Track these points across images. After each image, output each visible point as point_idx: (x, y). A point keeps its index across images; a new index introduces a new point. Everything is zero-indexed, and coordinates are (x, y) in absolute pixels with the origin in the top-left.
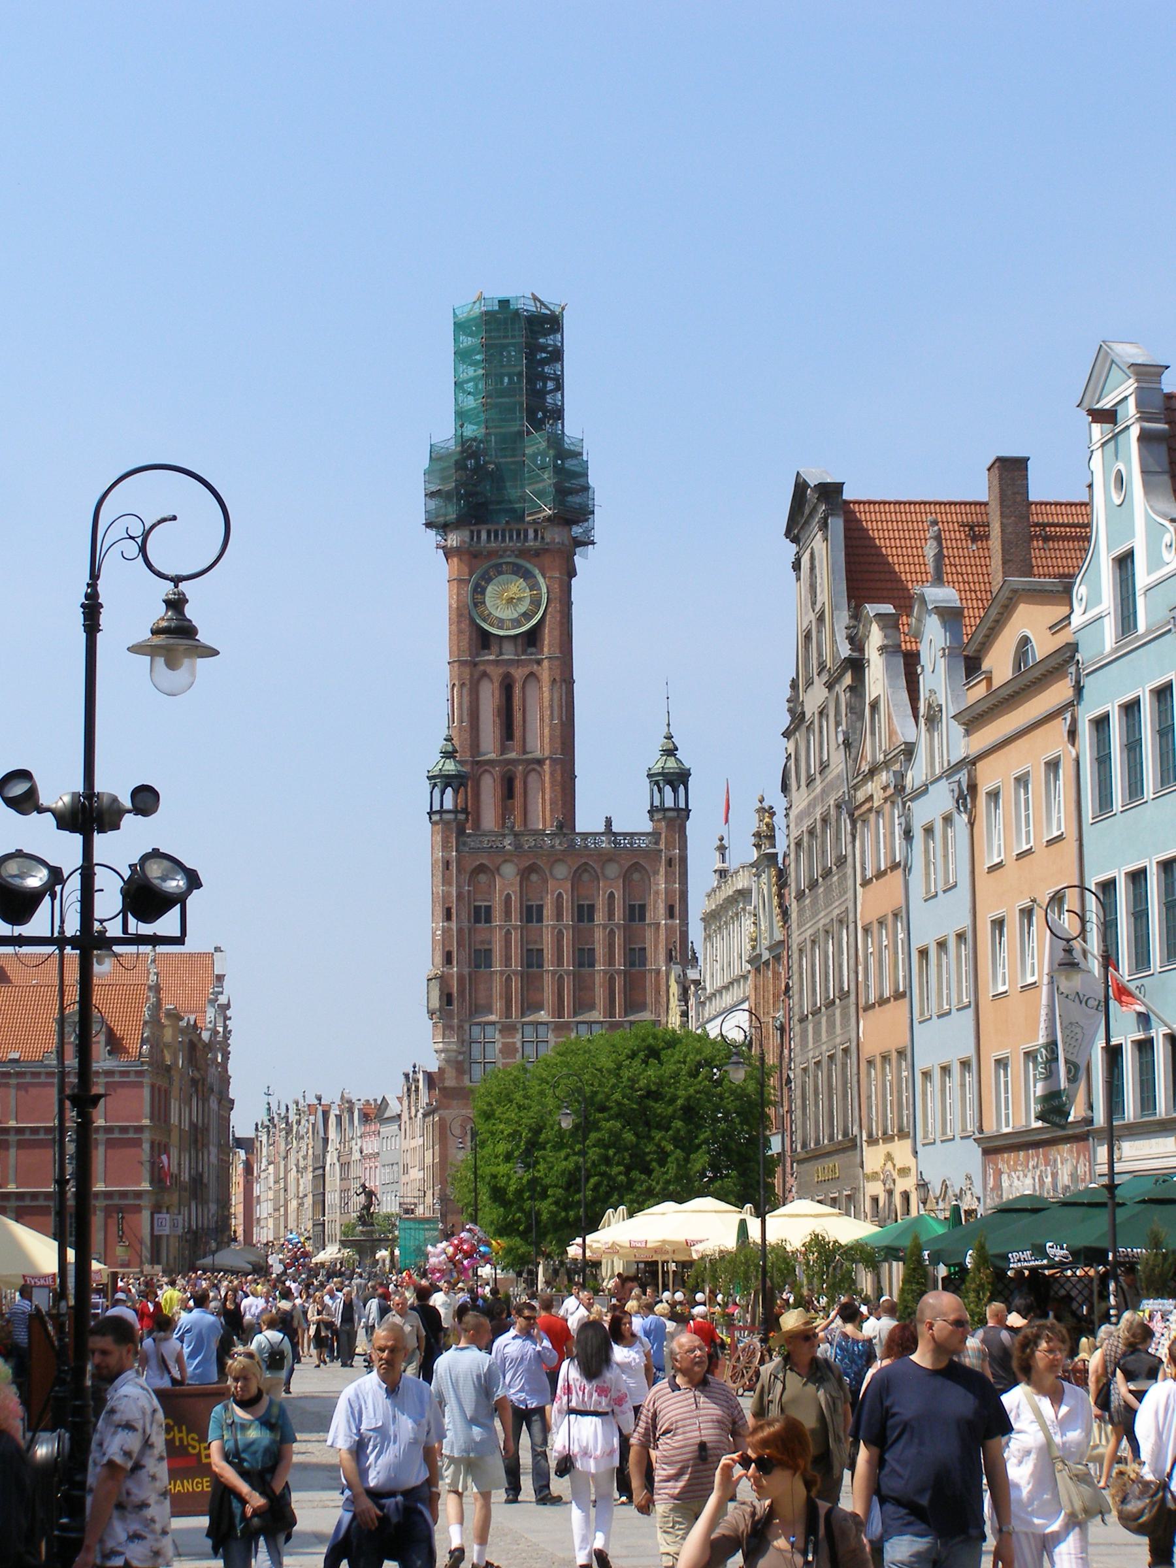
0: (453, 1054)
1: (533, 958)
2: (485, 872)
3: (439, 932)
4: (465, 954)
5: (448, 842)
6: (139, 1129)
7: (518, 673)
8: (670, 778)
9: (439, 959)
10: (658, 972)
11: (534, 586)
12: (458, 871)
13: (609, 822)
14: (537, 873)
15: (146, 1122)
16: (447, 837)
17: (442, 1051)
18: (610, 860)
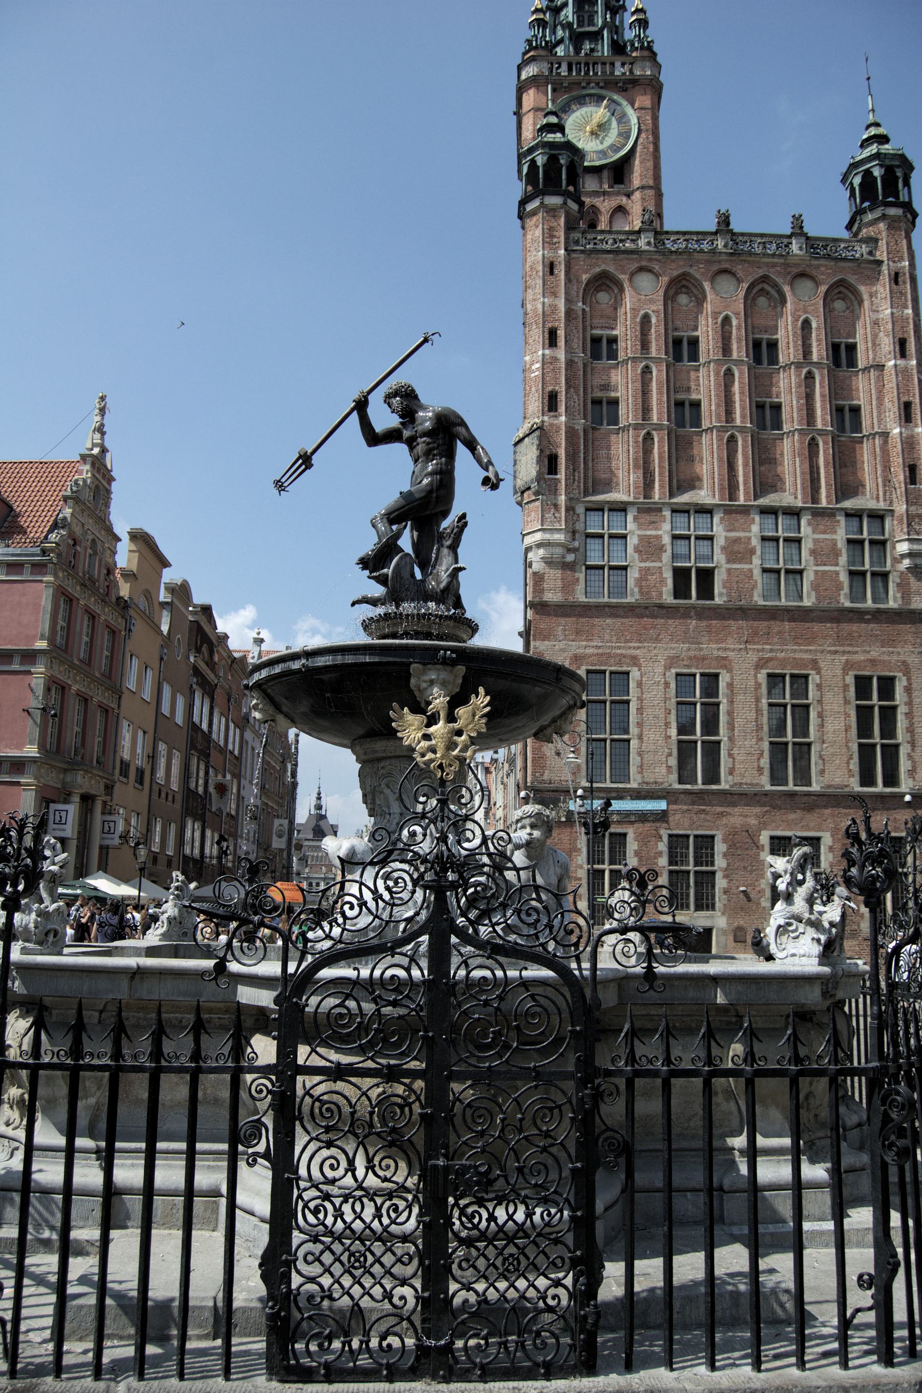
0: (559, 551)
1: (685, 411)
2: (608, 289)
3: (538, 365)
4: (578, 400)
5: (554, 236)
6: (30, 656)
7: (605, 206)
8: (887, 162)
9: (535, 404)
10: (885, 435)
11: (622, 119)
12: (568, 280)
13: (798, 223)
14: (689, 293)
15: (42, 644)
16: (551, 229)
17: (539, 545)
18: (803, 275)
